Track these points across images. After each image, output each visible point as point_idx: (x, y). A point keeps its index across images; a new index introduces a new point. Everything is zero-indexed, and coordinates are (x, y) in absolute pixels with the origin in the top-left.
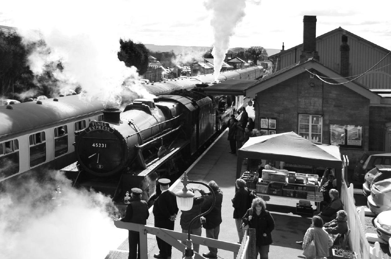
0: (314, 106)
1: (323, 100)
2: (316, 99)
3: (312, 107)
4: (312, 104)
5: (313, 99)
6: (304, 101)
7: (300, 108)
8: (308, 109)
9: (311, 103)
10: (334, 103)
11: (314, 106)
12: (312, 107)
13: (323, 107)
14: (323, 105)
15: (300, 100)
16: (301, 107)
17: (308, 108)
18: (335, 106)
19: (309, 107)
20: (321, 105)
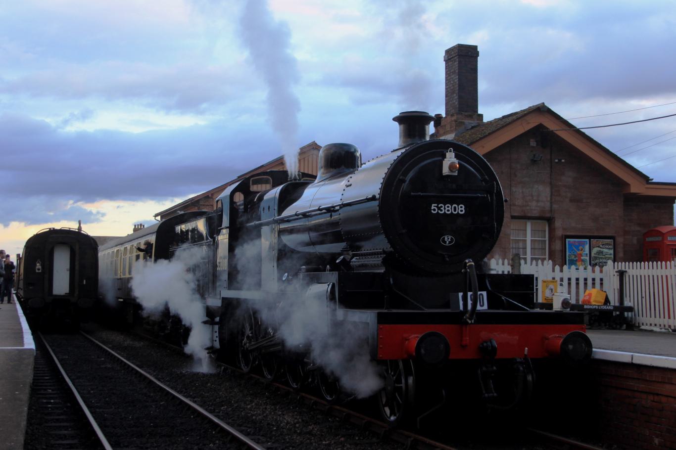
0: (538, 201)
1: (551, 188)
2: (541, 188)
3: (534, 203)
4: (535, 198)
5: (536, 186)
6: (521, 191)
7: (514, 205)
8: (528, 208)
9: (532, 196)
10: (569, 195)
11: (538, 201)
12: (534, 203)
13: (551, 203)
14: (551, 199)
15: (514, 190)
16: (517, 203)
17: (528, 205)
18: (571, 201)
19: (530, 203)
20: (549, 199)
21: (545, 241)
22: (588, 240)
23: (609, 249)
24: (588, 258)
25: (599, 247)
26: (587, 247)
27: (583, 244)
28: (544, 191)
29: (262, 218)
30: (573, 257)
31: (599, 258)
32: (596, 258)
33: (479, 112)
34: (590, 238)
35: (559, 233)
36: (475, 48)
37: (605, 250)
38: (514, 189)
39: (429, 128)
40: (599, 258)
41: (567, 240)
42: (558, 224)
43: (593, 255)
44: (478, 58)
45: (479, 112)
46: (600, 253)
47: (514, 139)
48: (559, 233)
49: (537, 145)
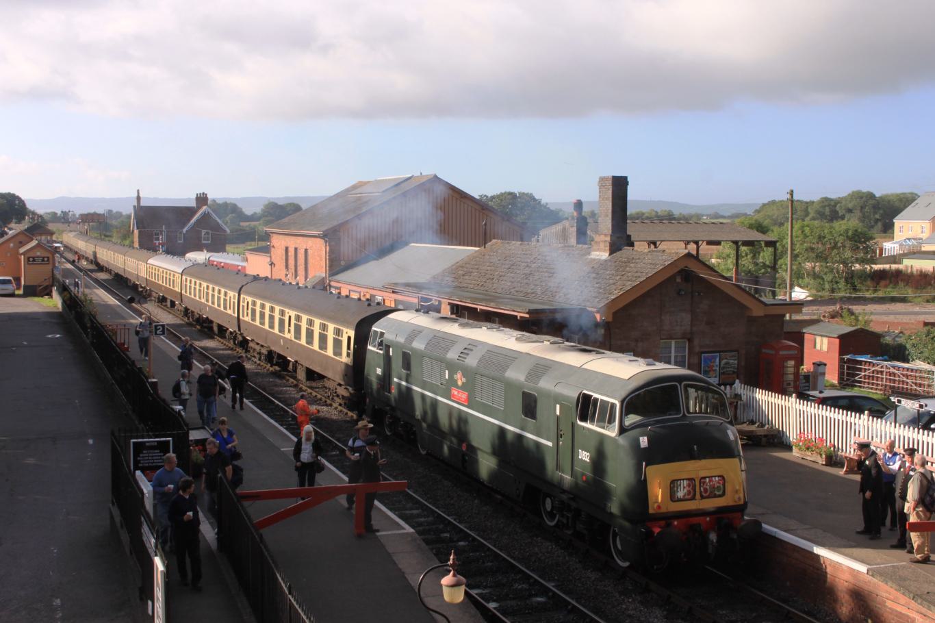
0: (681, 326)
11: (681, 326)
21: (685, 356)
22: (718, 354)
23: (734, 360)
24: (718, 368)
25: (726, 359)
26: (718, 360)
27: (715, 358)
28: (686, 318)
29: (442, 311)
30: (707, 369)
31: (726, 368)
32: (724, 368)
33: (628, 233)
34: (719, 352)
35: (697, 349)
36: (626, 178)
37: (732, 361)
38: (663, 317)
39: (631, 355)
40: (726, 368)
41: (703, 355)
42: (696, 342)
43: (722, 366)
44: (628, 187)
45: (628, 233)
46: (727, 363)
47: (664, 281)
48: (697, 349)
49: (682, 280)
